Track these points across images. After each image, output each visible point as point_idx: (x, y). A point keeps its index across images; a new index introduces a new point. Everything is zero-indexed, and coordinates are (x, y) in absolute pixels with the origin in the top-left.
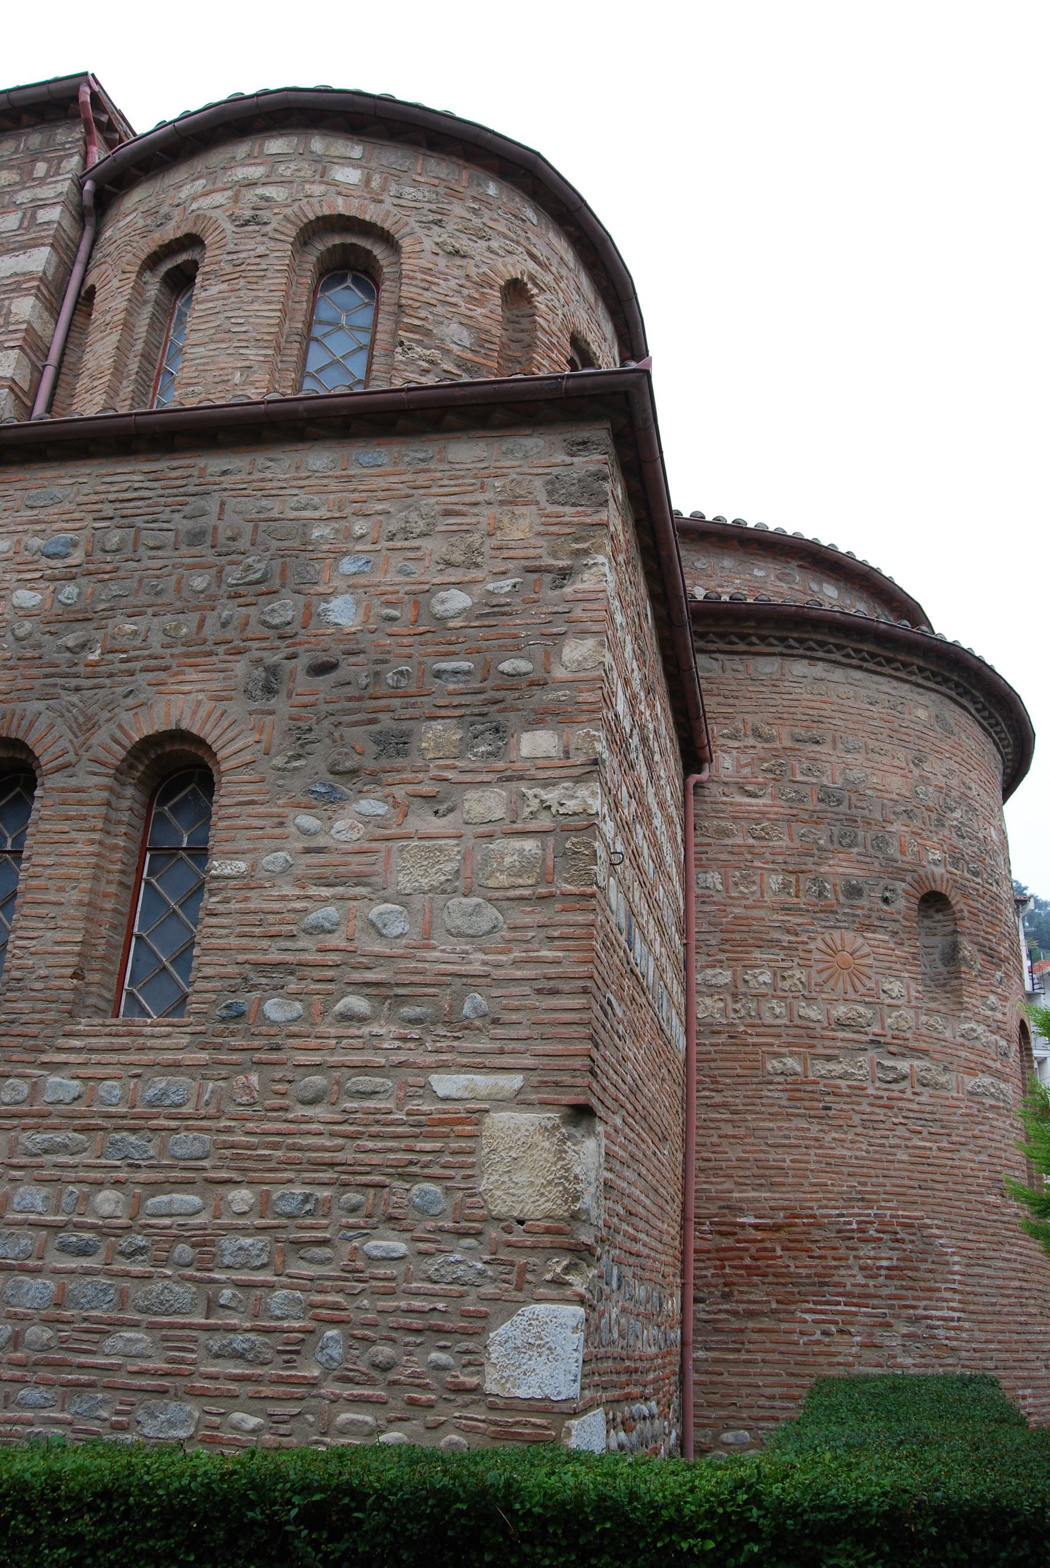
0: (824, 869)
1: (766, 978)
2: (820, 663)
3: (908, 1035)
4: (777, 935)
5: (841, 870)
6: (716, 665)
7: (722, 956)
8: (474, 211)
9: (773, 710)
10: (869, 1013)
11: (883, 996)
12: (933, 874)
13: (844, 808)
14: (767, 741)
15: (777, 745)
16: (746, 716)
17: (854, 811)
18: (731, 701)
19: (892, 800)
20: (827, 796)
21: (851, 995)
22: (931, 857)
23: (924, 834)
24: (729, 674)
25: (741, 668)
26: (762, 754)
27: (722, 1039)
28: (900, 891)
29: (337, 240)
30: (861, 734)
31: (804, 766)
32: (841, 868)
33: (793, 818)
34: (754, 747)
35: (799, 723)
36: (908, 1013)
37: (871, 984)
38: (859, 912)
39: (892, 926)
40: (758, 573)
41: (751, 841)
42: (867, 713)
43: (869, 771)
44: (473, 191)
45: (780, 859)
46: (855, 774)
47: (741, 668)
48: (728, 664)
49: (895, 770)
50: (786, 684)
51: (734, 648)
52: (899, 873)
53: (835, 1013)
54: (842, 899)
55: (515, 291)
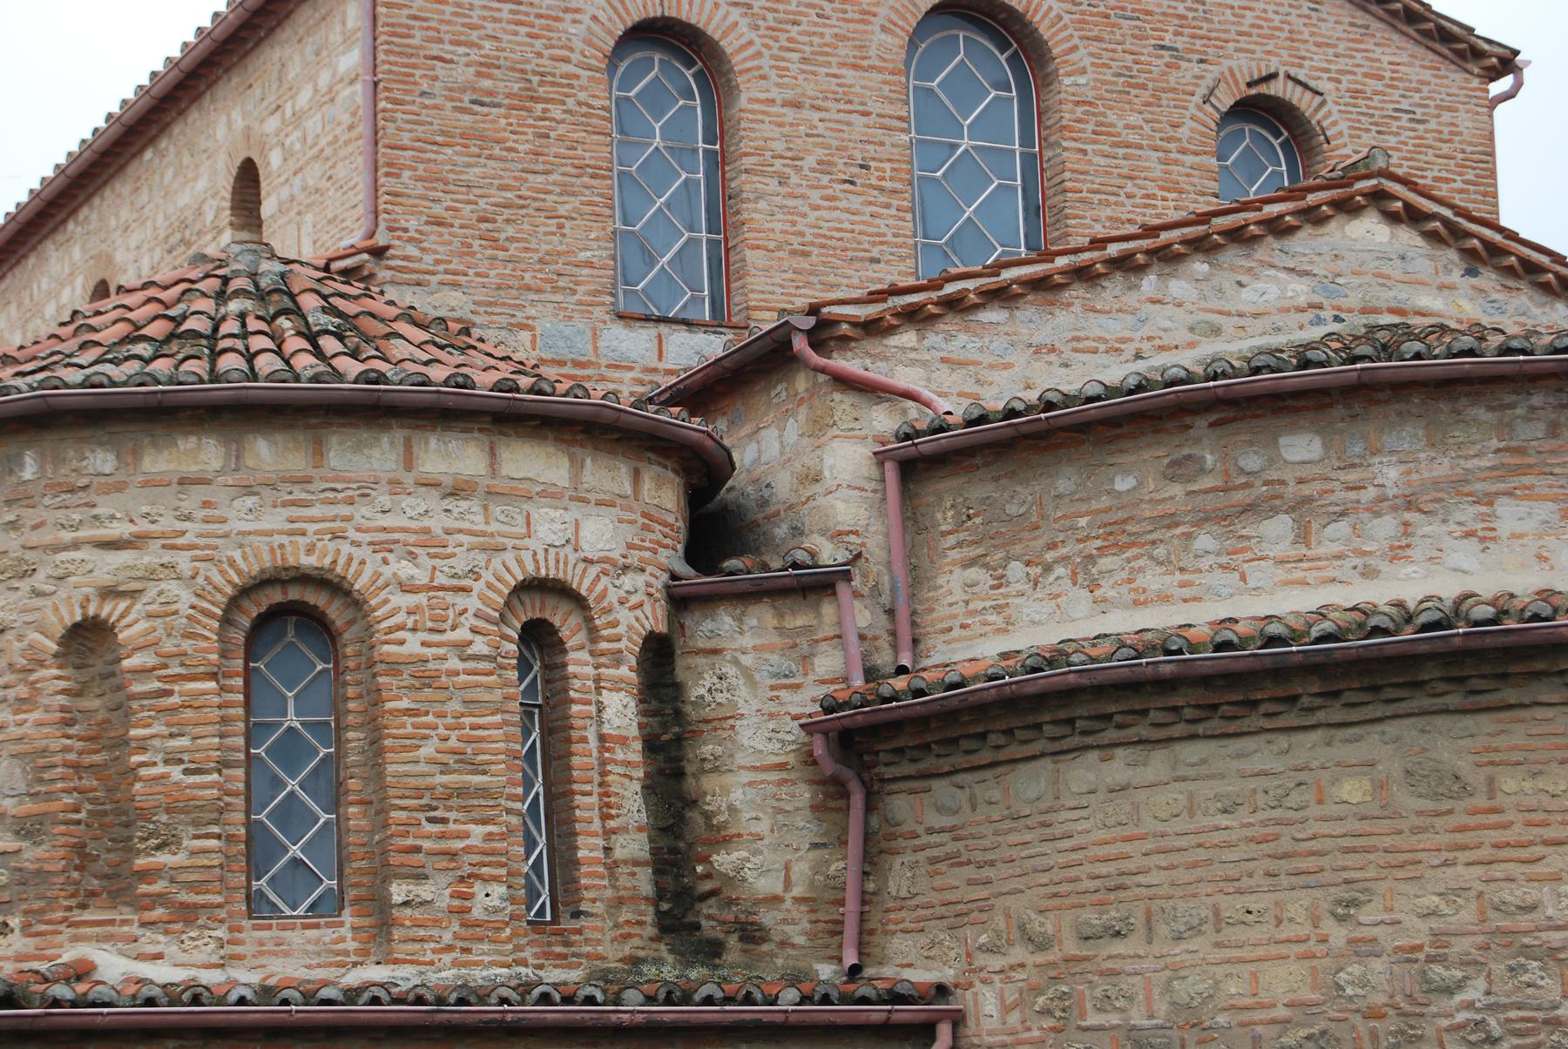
2: (1120, 752)
6: (962, 797)
9: (1044, 878)
15: (1054, 955)
16: (1009, 901)
18: (987, 872)
19: (1274, 1022)
24: (983, 809)
25: (996, 794)
26: (1035, 980)
30: (1205, 888)
31: (1098, 992)
34: (1022, 966)
35: (1086, 899)
40: (1123, 484)
42: (1217, 837)
43: (1219, 971)
46: (1191, 986)
47: (996, 794)
48: (978, 789)
49: (1283, 950)
50: (1064, 815)
51: (977, 759)
55: (87, 638)
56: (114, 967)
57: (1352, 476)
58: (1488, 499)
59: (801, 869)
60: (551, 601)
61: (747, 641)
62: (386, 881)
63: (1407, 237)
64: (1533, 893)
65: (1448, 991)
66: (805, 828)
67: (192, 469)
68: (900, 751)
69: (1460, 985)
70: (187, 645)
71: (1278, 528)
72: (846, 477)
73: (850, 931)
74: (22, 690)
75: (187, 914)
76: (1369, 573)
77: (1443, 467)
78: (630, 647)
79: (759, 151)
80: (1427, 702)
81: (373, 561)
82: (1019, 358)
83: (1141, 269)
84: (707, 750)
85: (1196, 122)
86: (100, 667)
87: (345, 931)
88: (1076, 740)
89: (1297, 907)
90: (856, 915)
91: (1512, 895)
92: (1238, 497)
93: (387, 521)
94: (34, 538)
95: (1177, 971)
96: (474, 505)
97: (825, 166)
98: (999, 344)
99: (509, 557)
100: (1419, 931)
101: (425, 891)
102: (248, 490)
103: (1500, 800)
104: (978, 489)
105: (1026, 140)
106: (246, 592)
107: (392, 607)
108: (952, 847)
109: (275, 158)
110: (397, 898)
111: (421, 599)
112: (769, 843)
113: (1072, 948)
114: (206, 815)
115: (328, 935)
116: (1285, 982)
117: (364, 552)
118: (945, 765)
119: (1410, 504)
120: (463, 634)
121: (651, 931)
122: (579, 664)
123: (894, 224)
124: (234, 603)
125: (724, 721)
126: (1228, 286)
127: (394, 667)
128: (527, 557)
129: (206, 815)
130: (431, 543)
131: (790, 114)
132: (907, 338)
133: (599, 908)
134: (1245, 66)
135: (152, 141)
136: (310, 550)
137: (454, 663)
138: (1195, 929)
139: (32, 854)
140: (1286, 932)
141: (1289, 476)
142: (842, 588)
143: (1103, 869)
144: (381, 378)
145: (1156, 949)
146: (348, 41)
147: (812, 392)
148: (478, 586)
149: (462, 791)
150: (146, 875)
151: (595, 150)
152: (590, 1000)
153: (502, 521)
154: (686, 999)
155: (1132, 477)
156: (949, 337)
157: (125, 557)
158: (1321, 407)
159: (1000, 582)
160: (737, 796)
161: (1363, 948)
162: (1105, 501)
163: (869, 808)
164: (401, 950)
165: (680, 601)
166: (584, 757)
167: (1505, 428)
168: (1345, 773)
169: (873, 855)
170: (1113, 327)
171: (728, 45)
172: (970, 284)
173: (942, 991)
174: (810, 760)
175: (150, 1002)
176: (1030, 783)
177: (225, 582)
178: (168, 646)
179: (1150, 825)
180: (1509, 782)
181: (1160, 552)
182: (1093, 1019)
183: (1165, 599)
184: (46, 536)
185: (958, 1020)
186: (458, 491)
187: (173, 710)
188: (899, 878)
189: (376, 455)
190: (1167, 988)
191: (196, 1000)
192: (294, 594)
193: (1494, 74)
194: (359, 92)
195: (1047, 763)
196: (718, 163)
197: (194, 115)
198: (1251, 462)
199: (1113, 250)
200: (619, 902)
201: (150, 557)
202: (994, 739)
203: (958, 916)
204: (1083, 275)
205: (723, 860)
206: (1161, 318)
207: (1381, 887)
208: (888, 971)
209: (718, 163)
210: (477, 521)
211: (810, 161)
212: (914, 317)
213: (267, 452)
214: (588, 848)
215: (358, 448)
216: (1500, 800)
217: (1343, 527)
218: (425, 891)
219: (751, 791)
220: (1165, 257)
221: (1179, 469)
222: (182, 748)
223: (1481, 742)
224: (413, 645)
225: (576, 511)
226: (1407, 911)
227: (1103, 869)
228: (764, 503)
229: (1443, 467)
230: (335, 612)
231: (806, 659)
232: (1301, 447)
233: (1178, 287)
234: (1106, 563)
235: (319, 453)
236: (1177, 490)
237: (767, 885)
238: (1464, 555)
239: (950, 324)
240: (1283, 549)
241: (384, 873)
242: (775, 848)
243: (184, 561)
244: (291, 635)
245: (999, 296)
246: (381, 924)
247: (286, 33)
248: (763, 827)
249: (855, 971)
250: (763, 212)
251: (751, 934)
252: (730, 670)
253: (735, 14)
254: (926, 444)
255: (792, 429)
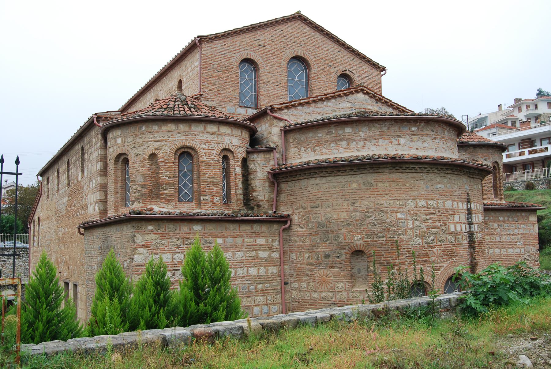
0: (319, 250)
1: (305, 286)
3: (345, 300)
4: (307, 272)
5: (323, 250)
6: (293, 185)
7: (296, 279)
8: (141, 138)
10: (331, 294)
11: (336, 288)
12: (357, 244)
13: (325, 228)
14: (305, 209)
15: (306, 210)
17: (328, 229)
18: (296, 197)
20: (320, 225)
21: (326, 289)
22: (356, 238)
23: (354, 231)
27: (297, 303)
28: (343, 253)
29: (121, 160)
32: (323, 249)
33: (311, 235)
36: (344, 294)
37: (332, 285)
38: (329, 263)
39: (340, 265)
40: (320, 135)
41: (301, 243)
42: (333, 192)
44: (140, 132)
45: (307, 248)
52: (343, 247)
53: (322, 295)
54: (323, 259)
55: (153, 156)
56: (156, 209)
57: (356, 135)
58: (378, 139)
59: (267, 196)
60: (227, 152)
61: (259, 159)
62: (200, 196)
63: (367, 97)
64: (383, 202)
65: (369, 217)
66: (268, 189)
67: (170, 129)
68: (283, 177)
69: (371, 216)
70: (169, 158)
71: (344, 143)
72: (276, 133)
73: (274, 206)
74: (142, 164)
75: (168, 201)
76: (359, 151)
77: (371, 134)
78: (240, 160)
79: (263, 80)
80: (367, 171)
81: (199, 145)
82: (304, 114)
83: (324, 101)
84: (252, 176)
85: (334, 77)
86: (155, 161)
87: (194, 204)
88: (311, 176)
89: (345, 203)
90: (275, 203)
91: (379, 202)
92: (338, 138)
93: (201, 138)
94: (144, 140)
95: (326, 213)
96: (215, 136)
97: (274, 83)
98: (300, 112)
99: (221, 145)
100: (364, 208)
101: (206, 198)
102: (179, 133)
103: (378, 187)
104: (297, 136)
105: (306, 79)
106: (178, 149)
107: (202, 152)
108: (291, 193)
109: (185, 79)
110: (202, 199)
111: (207, 151)
112: (262, 191)
113: (309, 209)
114: (171, 185)
115: (191, 204)
116: (343, 215)
117: (198, 143)
118: (290, 180)
119: (365, 140)
120: (213, 157)
121: (242, 205)
122: (232, 162)
123: (285, 93)
124: (176, 151)
125: (255, 172)
126: (338, 104)
127: (202, 162)
128: (224, 145)
129: (171, 185)
130: (208, 142)
131: (268, 74)
132: (286, 111)
133: (234, 201)
134: (342, 69)
135: (165, 76)
136: (189, 143)
137: (212, 162)
138: (329, 207)
139: (144, 191)
140: (344, 207)
141: (346, 135)
142: (274, 151)
143: (315, 197)
144: (201, 115)
145: (323, 210)
146: (197, 60)
147: (270, 119)
148: (216, 149)
149: (212, 182)
150: (162, 194)
151: (237, 79)
152: (233, 216)
153: (220, 139)
154: (248, 216)
155: (321, 134)
156: (293, 111)
157: (159, 143)
158: (351, 124)
159: (300, 151)
160: (257, 184)
161: (355, 210)
162: (317, 138)
163: (278, 186)
164: (202, 207)
165: (248, 153)
166: (232, 177)
167: (381, 128)
168: (354, 182)
169: (278, 194)
170: (319, 110)
171: (258, 63)
172: (296, 102)
173: (289, 216)
174: (268, 178)
175: (162, 214)
176: (303, 183)
177: (175, 148)
178: (166, 158)
179: (322, 190)
180: (379, 184)
181: (325, 146)
182: (312, 221)
183: (326, 154)
184: (146, 140)
185: (291, 220)
186: (213, 134)
187: (166, 168)
188: (282, 197)
189: (200, 128)
190: (324, 216)
191: (169, 214)
192: (186, 150)
193: (382, 71)
194: (198, 69)
195: (306, 180)
196: (256, 82)
197: (172, 72)
198: (340, 132)
199: (319, 97)
200: (238, 200)
201: (163, 143)
202: (298, 176)
203: (292, 204)
204: (314, 101)
205: (254, 194)
206: (327, 108)
207: (359, 201)
208: (280, 212)
209: (256, 82)
210: (216, 139)
211: (271, 82)
212: (287, 107)
213: (182, 127)
214: (233, 192)
215: (197, 126)
216: (378, 187)
217: (355, 143)
218: (206, 198)
219: (259, 184)
220: (328, 99)
221: (329, 133)
222: (168, 174)
223: (375, 178)
224: (205, 158)
225: (232, 138)
226: (362, 204)
227: (315, 197)
228: (262, 137)
229: (371, 134)
230: (193, 153)
231: (268, 162)
232: (348, 130)
233: (330, 104)
234: (317, 148)
235: (190, 127)
236: (328, 136)
237: (261, 198)
238: (374, 148)
239: (293, 109)
240: (345, 146)
241: (200, 195)
242: (263, 192)
243: (168, 144)
244: (185, 156)
245: (301, 104)
246: (199, 203)
247: (187, 59)
248: (261, 189)
249: (275, 212)
250: (263, 90)
251: (259, 206)
252: (256, 164)
253: (260, 58)
254: (288, 128)
255: (267, 125)
